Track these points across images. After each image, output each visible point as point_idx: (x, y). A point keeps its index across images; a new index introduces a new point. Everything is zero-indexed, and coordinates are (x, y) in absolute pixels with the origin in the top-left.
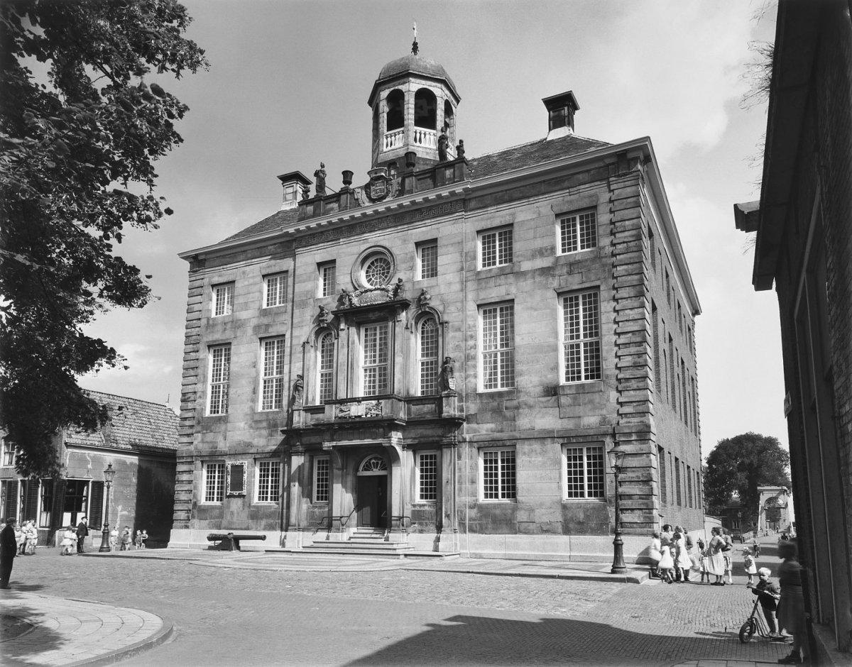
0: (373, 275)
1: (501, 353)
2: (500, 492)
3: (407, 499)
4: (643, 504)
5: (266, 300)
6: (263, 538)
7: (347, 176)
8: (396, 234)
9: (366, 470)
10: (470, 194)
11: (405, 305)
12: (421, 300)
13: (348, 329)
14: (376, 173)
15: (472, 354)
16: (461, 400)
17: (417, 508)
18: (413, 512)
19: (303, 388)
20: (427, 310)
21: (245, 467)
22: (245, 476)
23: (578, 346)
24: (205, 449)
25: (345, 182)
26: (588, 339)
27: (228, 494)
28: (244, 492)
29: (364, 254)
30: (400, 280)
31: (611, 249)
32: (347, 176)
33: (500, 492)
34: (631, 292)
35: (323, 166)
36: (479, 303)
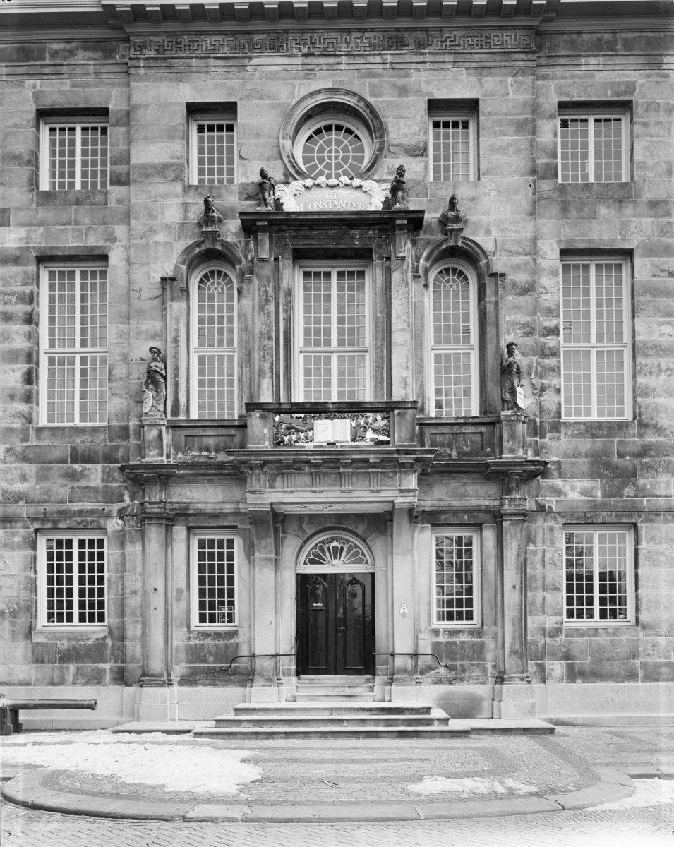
3: (423, 619)
10: (551, 20)
12: (451, 220)
13: (276, 259)
15: (551, 345)
17: (443, 639)
18: (436, 646)
19: (165, 378)
20: (460, 244)
29: (311, 103)
30: (401, 171)
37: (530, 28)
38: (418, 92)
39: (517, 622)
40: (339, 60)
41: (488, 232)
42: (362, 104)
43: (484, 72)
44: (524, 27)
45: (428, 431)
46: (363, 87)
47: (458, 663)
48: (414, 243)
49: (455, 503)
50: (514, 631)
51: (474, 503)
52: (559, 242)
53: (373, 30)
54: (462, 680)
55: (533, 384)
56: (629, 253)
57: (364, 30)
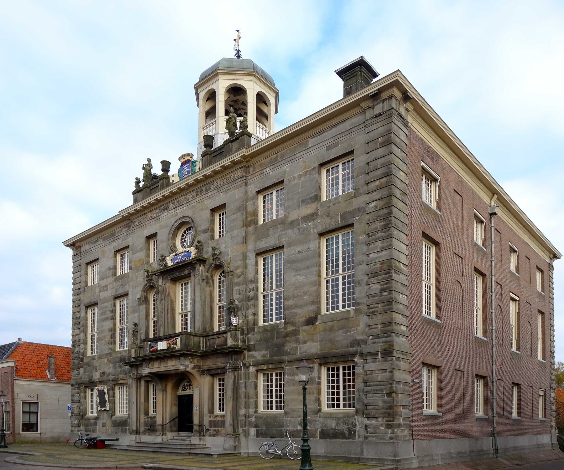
0: (185, 241)
1: (276, 293)
2: (274, 405)
4: (385, 413)
5: (120, 270)
6: (117, 440)
7: (166, 165)
8: (181, 210)
9: (184, 390)
11: (201, 261)
14: (184, 159)
16: (242, 334)
21: (106, 391)
22: (107, 397)
23: (338, 279)
24: (86, 379)
25: (163, 170)
26: (347, 273)
27: (99, 410)
28: (108, 408)
31: (366, 187)
32: (166, 165)
33: (274, 405)
34: (379, 224)
35: (149, 160)
36: (258, 252)
37: (242, 167)
38: (207, 208)
39: (232, 412)
40: (183, 206)
41: (228, 254)
42: (190, 219)
43: (228, 191)
44: (241, 168)
45: (207, 338)
46: (189, 213)
47: (217, 429)
48: (204, 266)
49: (214, 366)
50: (231, 416)
51: (220, 365)
52: (255, 251)
53: (193, 191)
54: (218, 435)
55: (243, 314)
56: (282, 247)
57: (191, 192)
